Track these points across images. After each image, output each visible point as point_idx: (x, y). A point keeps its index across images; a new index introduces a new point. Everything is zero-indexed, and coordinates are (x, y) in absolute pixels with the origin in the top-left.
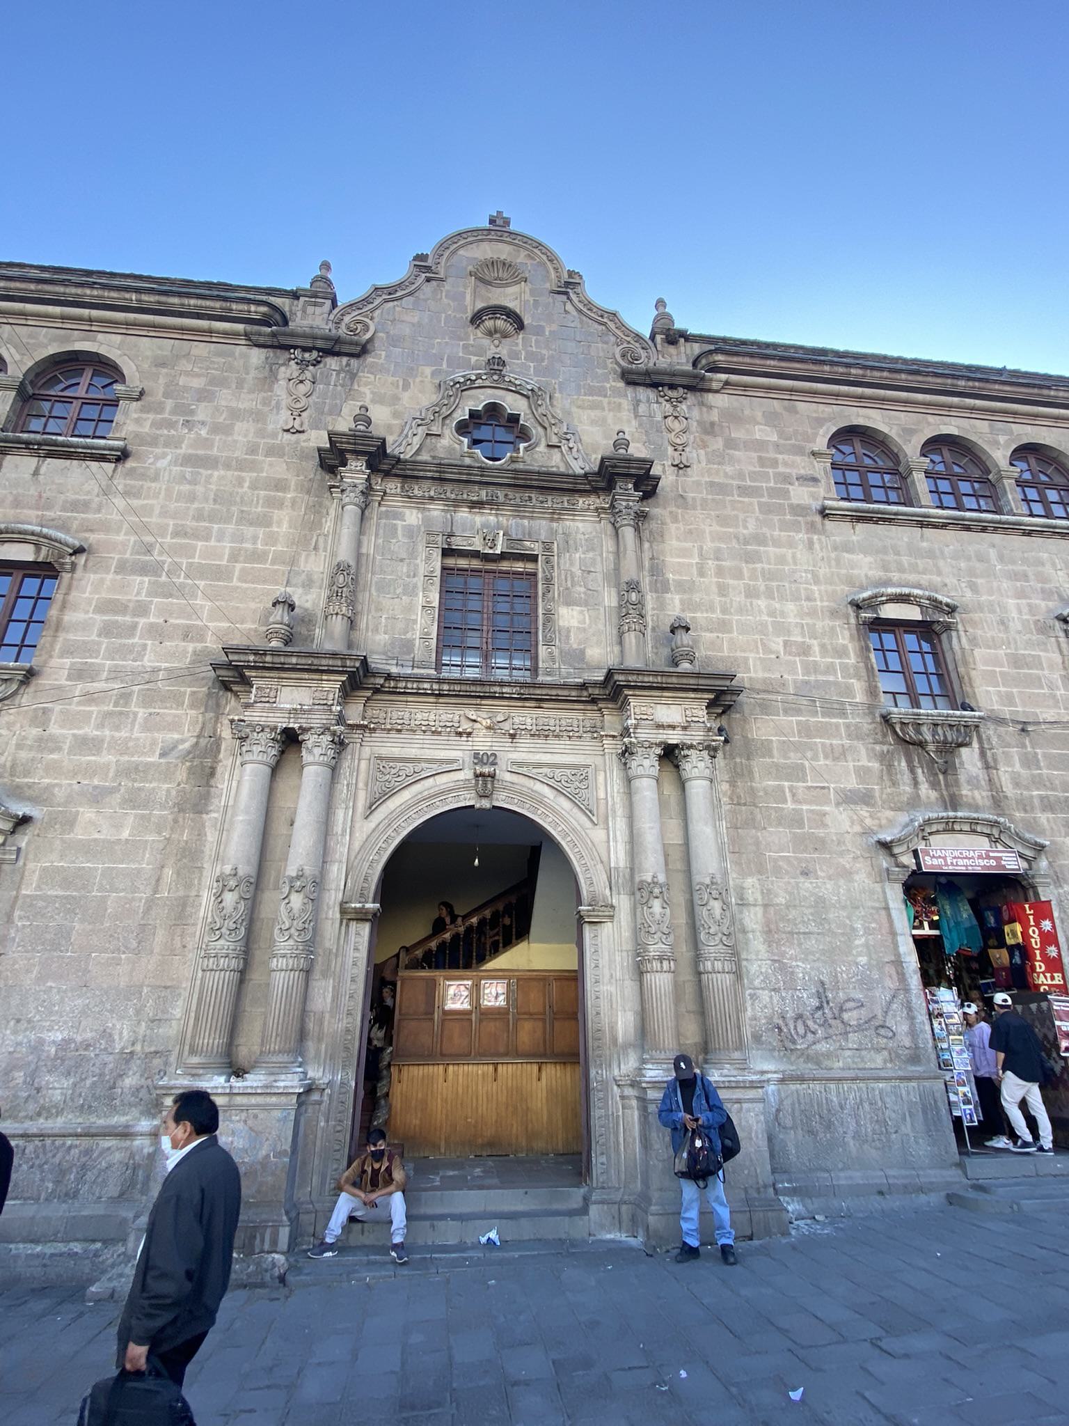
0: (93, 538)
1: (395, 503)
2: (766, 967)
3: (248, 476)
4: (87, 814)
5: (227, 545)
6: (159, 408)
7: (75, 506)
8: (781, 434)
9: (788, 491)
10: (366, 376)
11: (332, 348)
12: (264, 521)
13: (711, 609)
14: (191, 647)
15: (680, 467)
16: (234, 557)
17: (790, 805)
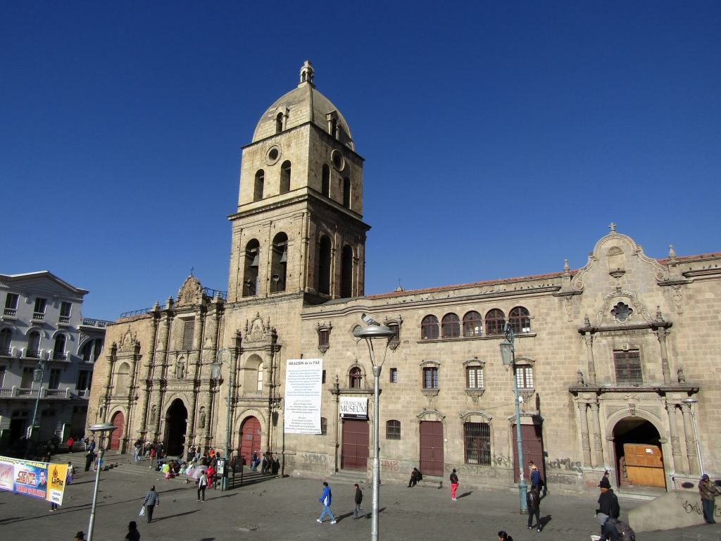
0: (536, 357)
1: (599, 338)
2: (709, 454)
3: (563, 336)
4: (553, 418)
5: (563, 355)
6: (539, 320)
7: (531, 349)
8: (716, 295)
9: (717, 316)
10: (584, 300)
11: (574, 294)
12: (569, 348)
13: (692, 360)
14: (562, 382)
15: (680, 314)
16: (566, 358)
17: (716, 416)
